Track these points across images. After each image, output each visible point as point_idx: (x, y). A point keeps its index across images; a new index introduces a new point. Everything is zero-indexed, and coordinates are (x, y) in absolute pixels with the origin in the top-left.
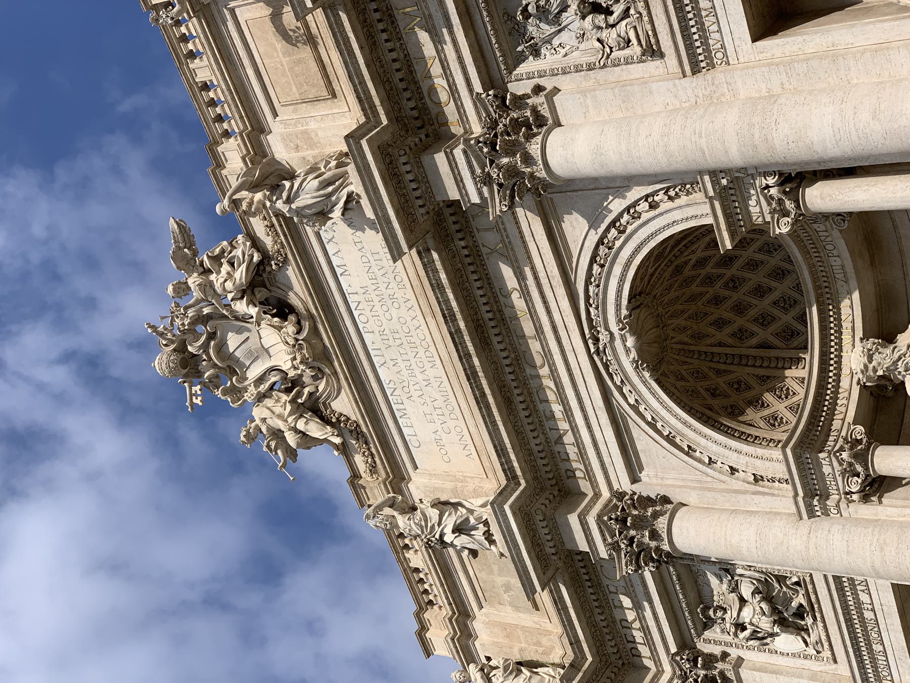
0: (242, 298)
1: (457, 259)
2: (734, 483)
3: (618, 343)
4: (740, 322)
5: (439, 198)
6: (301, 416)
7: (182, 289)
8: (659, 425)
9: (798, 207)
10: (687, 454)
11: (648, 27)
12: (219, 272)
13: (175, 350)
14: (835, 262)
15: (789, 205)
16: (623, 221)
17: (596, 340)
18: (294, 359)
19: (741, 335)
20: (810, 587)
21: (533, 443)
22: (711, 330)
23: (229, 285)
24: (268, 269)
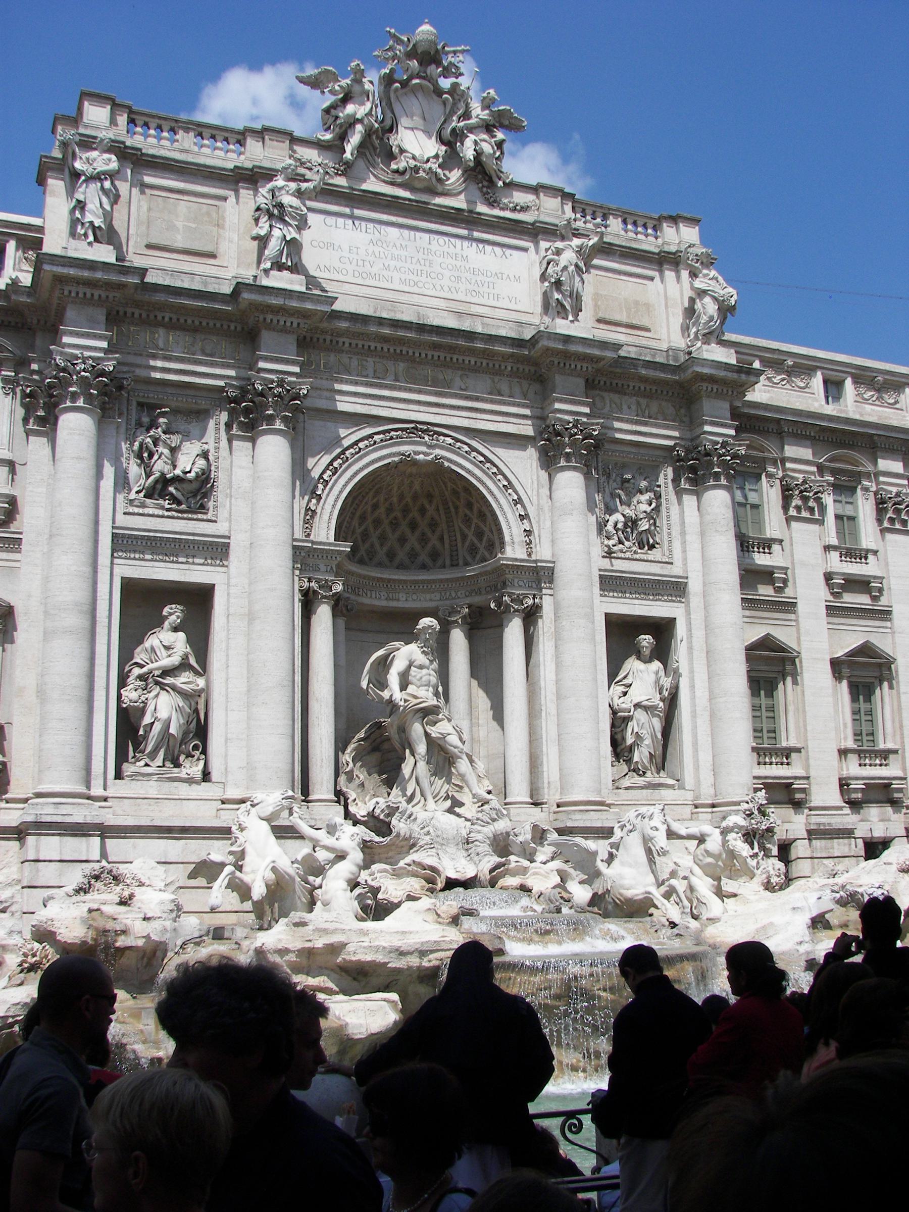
0: (475, 150)
1: (500, 359)
3: (423, 449)
4: (370, 519)
5: (558, 379)
8: (352, 450)
9: (518, 611)
13: (437, 51)
14: (402, 596)
16: (510, 491)
17: (423, 431)
18: (414, 158)
19: (363, 518)
20: (200, 516)
21: (347, 341)
22: (375, 501)
24: (486, 183)
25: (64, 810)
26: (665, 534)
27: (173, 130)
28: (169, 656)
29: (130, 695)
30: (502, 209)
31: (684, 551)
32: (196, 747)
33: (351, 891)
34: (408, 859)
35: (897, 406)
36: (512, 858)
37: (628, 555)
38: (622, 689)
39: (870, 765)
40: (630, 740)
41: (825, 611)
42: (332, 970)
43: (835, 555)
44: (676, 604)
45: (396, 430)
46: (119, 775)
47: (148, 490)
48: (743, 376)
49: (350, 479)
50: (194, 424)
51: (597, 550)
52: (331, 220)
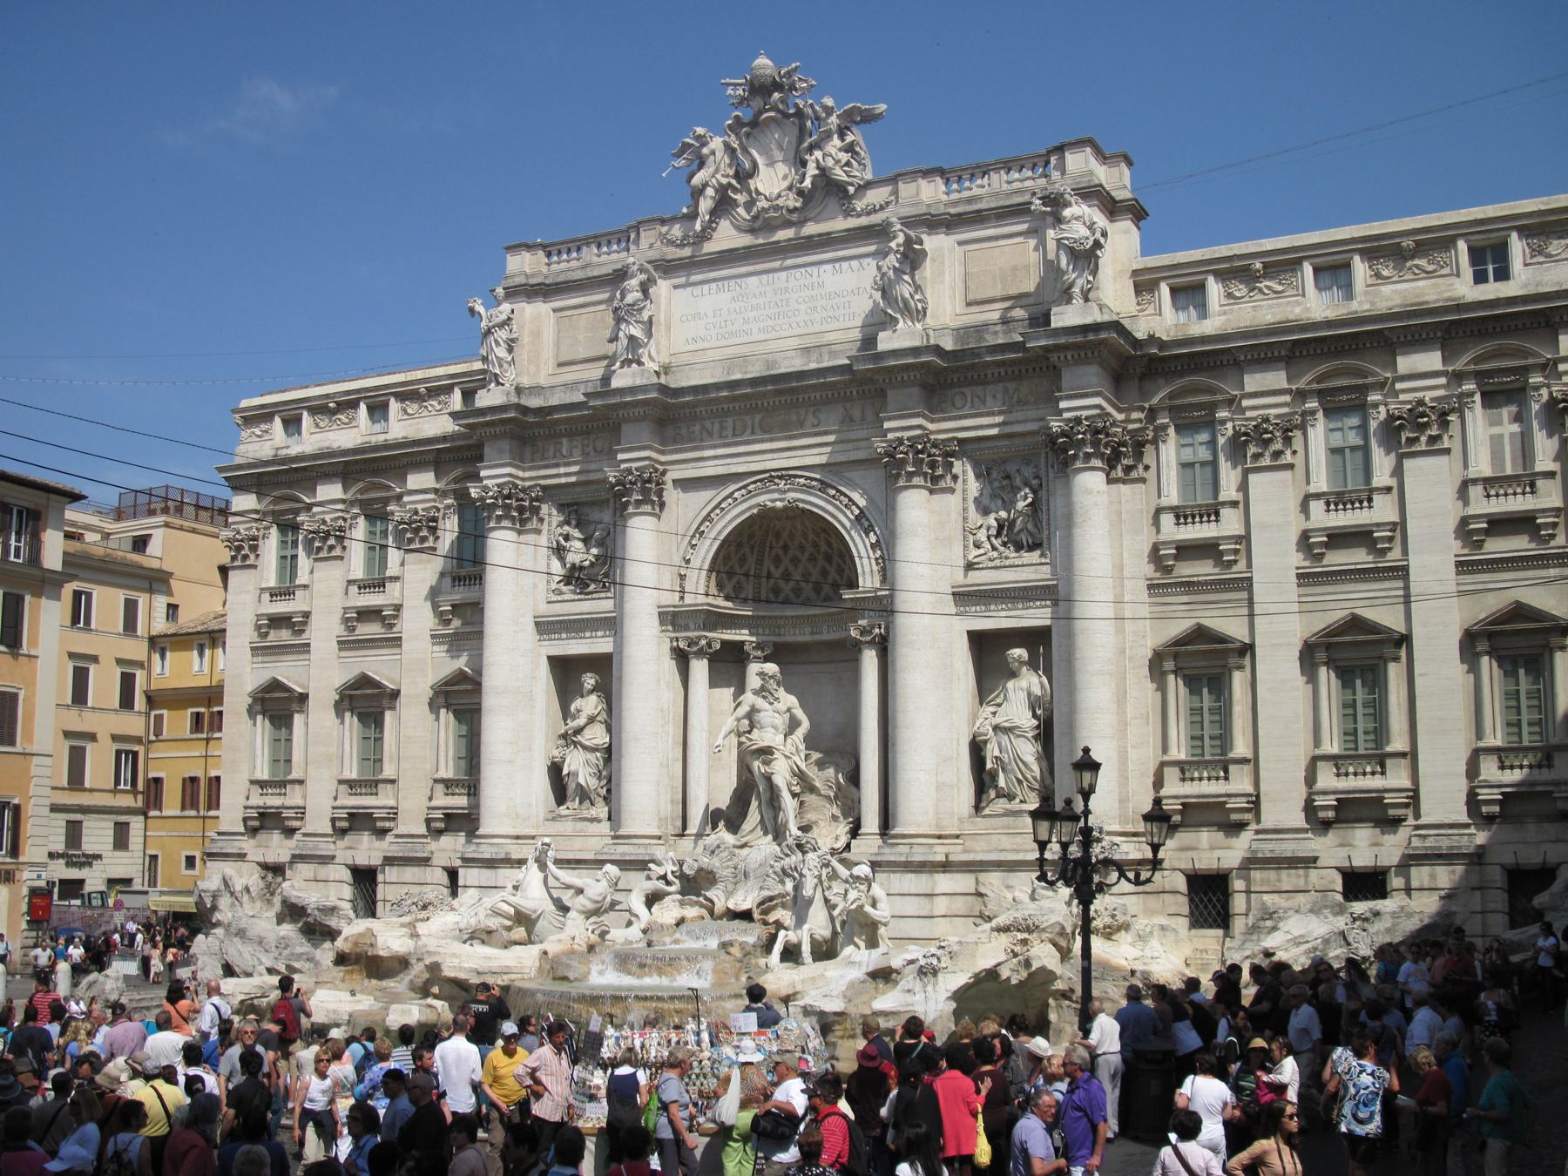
0: (818, 167)
2: (677, 560)
4: (786, 562)
6: (717, 191)
7: (829, 111)
12: (840, 150)
17: (780, 478)
19: (777, 561)
23: (830, 162)
25: (483, 848)
27: (579, 249)
29: (556, 753)
30: (859, 216)
35: (1446, 271)
37: (997, 563)
38: (992, 709)
39: (1355, 774)
40: (989, 765)
41: (1295, 580)
48: (1091, 337)
52: (697, 290)
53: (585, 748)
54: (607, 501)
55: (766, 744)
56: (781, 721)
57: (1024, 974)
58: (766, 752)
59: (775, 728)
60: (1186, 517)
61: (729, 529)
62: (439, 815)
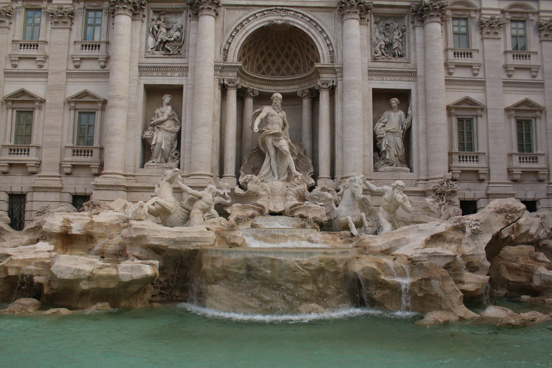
3: (280, 18)
4: (266, 54)
8: (246, 22)
9: (325, 89)
10: (236, 29)
11: (381, 60)
15: (326, 87)
17: (280, 10)
19: (262, 54)
20: (178, 56)
22: (266, 45)
26: (407, 49)
28: (163, 116)
31: (416, 57)
32: (176, 154)
33: (204, 213)
34: (254, 202)
36: (306, 202)
37: (385, 60)
39: (527, 162)
40: (384, 148)
41: (502, 84)
42: (146, 248)
43: (510, 56)
44: (412, 83)
45: (267, 10)
46: (142, 166)
47: (157, 47)
49: (244, 34)
50: (179, 18)
51: (367, 58)
53: (167, 131)
54: (181, 13)
55: (278, 131)
56: (281, 122)
57: (518, 235)
58: (276, 135)
59: (279, 124)
60: (458, 54)
61: (252, 30)
62: (69, 165)
